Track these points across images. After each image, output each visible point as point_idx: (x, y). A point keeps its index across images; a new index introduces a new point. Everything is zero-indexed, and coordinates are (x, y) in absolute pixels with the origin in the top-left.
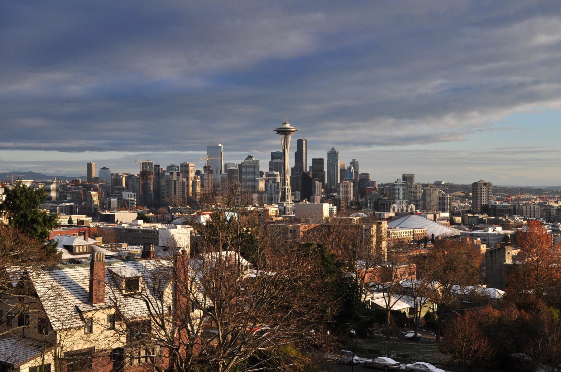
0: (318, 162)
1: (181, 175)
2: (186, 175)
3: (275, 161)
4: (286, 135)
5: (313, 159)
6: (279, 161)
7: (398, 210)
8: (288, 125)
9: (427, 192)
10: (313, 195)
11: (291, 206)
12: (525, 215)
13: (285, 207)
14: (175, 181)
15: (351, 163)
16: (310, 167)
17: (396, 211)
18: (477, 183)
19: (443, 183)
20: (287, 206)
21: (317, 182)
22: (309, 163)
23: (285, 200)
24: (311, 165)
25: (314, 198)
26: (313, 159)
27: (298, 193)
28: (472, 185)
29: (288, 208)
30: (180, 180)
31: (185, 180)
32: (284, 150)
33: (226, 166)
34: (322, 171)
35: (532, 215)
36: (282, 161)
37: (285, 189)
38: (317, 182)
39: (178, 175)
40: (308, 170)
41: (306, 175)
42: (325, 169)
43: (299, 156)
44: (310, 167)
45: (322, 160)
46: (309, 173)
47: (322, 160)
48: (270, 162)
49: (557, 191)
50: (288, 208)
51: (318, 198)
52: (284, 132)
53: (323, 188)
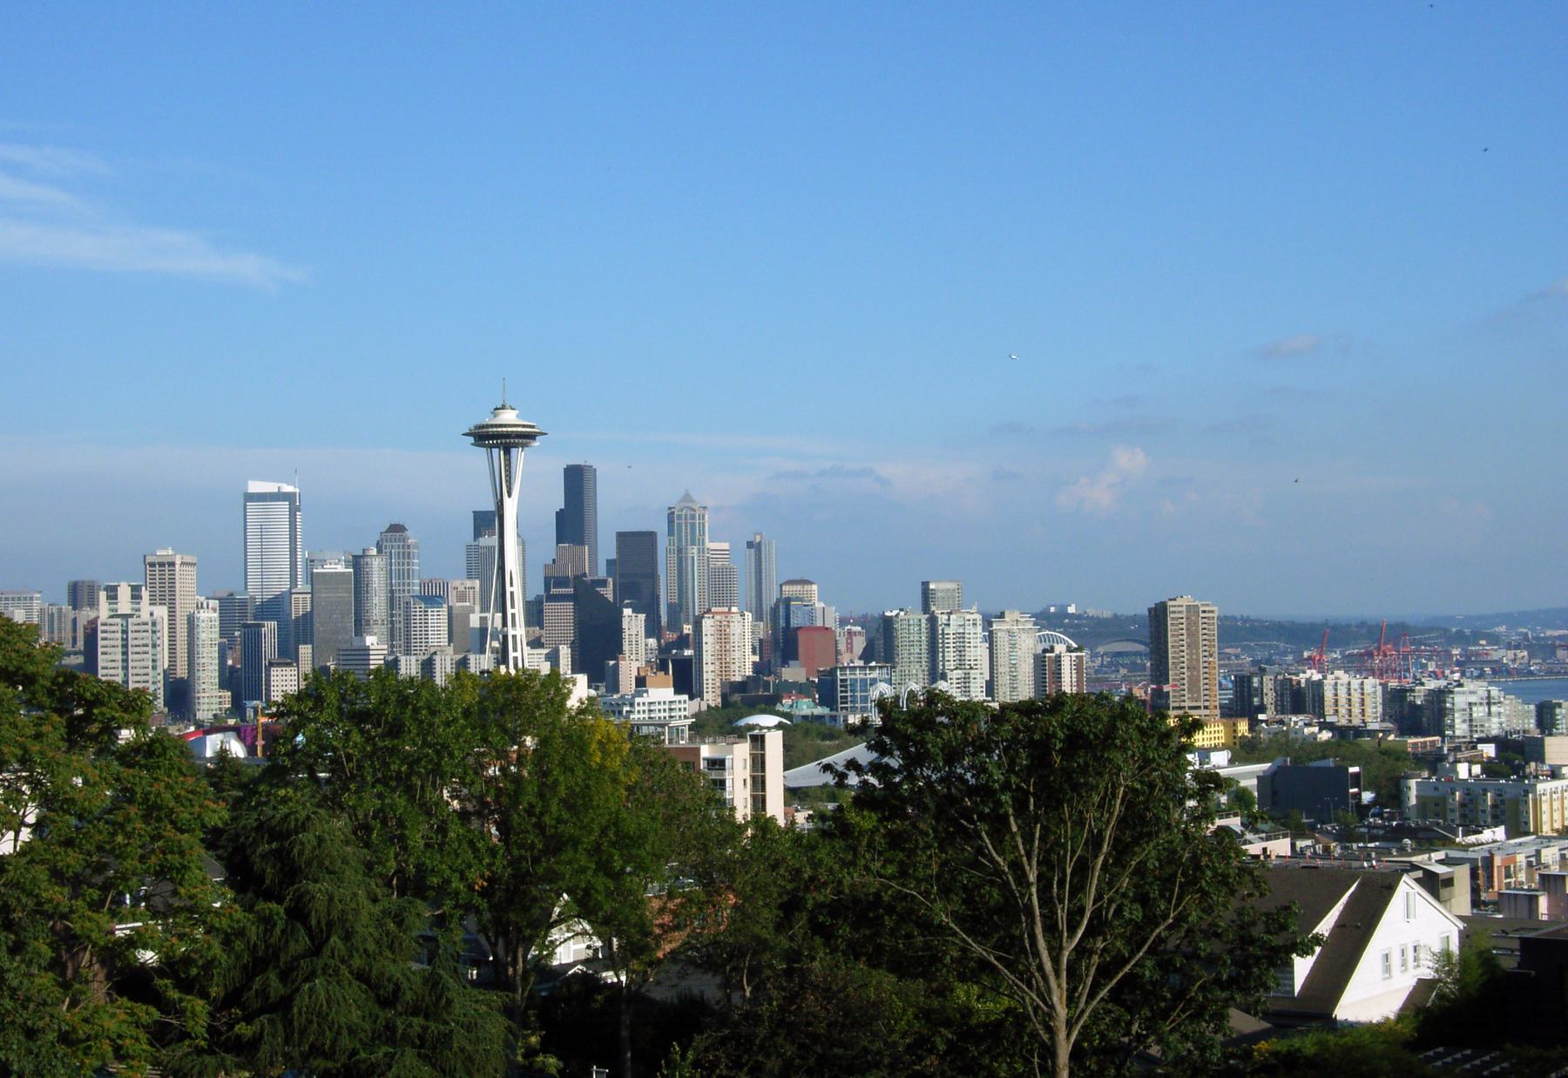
0: (636, 546)
1: (145, 594)
2: (165, 595)
4: (507, 452)
5: (621, 536)
8: (509, 417)
9: (1002, 640)
10: (616, 658)
12: (1329, 709)
14: (125, 617)
15: (750, 545)
19: (1071, 610)
21: (627, 612)
22: (607, 549)
24: (613, 555)
25: (616, 667)
26: (621, 536)
27: (565, 653)
30: (145, 616)
31: (162, 612)
33: (311, 562)
34: (653, 576)
35: (1356, 710)
36: (493, 541)
38: (627, 612)
39: (136, 596)
40: (602, 573)
43: (573, 522)
44: (610, 563)
46: (603, 583)
49: (1460, 632)
51: (629, 667)
53: (653, 629)
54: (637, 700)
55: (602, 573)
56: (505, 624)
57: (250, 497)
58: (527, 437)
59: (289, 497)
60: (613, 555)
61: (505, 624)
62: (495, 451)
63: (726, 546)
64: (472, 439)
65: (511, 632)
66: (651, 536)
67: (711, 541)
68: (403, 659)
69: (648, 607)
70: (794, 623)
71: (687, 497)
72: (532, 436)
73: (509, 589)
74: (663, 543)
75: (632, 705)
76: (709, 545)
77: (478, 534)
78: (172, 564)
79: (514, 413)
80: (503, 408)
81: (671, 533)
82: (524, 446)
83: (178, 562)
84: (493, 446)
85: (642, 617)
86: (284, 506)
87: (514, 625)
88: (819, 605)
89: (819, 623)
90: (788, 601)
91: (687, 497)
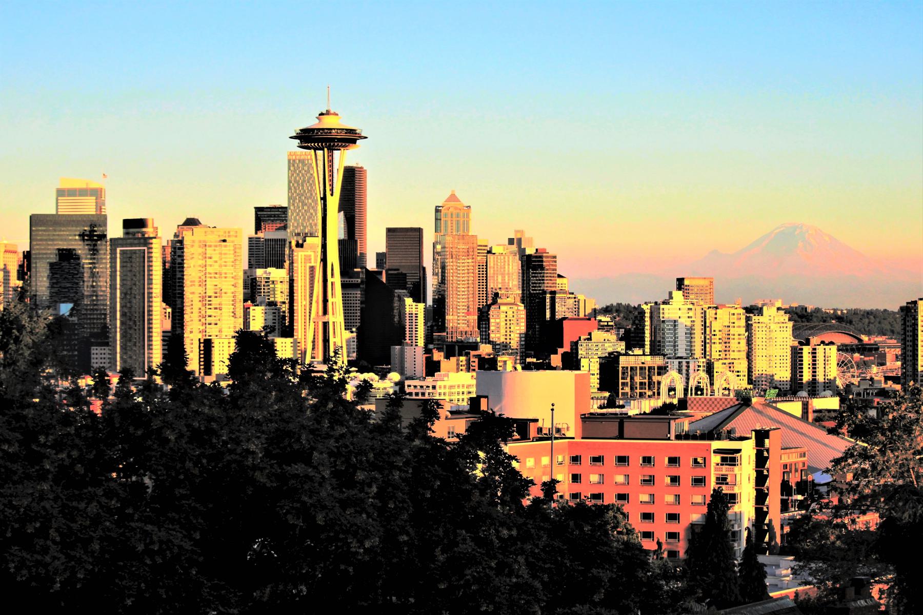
0: (405, 239)
5: (390, 231)
7: (686, 390)
15: (511, 241)
16: (378, 255)
17: (680, 394)
18: (915, 303)
22: (374, 244)
25: (402, 353)
26: (390, 231)
28: (902, 309)
32: (324, 199)
40: (371, 265)
42: (428, 261)
44: (378, 255)
45: (419, 231)
47: (419, 231)
56: (325, 312)
57: (61, 193)
59: (97, 193)
60: (383, 249)
61: (325, 312)
62: (320, 153)
65: (330, 318)
69: (419, 296)
70: (558, 316)
71: (453, 198)
72: (354, 141)
74: (429, 238)
75: (434, 387)
77: (258, 228)
80: (328, 113)
84: (315, 149)
85: (421, 306)
86: (92, 200)
91: (453, 198)
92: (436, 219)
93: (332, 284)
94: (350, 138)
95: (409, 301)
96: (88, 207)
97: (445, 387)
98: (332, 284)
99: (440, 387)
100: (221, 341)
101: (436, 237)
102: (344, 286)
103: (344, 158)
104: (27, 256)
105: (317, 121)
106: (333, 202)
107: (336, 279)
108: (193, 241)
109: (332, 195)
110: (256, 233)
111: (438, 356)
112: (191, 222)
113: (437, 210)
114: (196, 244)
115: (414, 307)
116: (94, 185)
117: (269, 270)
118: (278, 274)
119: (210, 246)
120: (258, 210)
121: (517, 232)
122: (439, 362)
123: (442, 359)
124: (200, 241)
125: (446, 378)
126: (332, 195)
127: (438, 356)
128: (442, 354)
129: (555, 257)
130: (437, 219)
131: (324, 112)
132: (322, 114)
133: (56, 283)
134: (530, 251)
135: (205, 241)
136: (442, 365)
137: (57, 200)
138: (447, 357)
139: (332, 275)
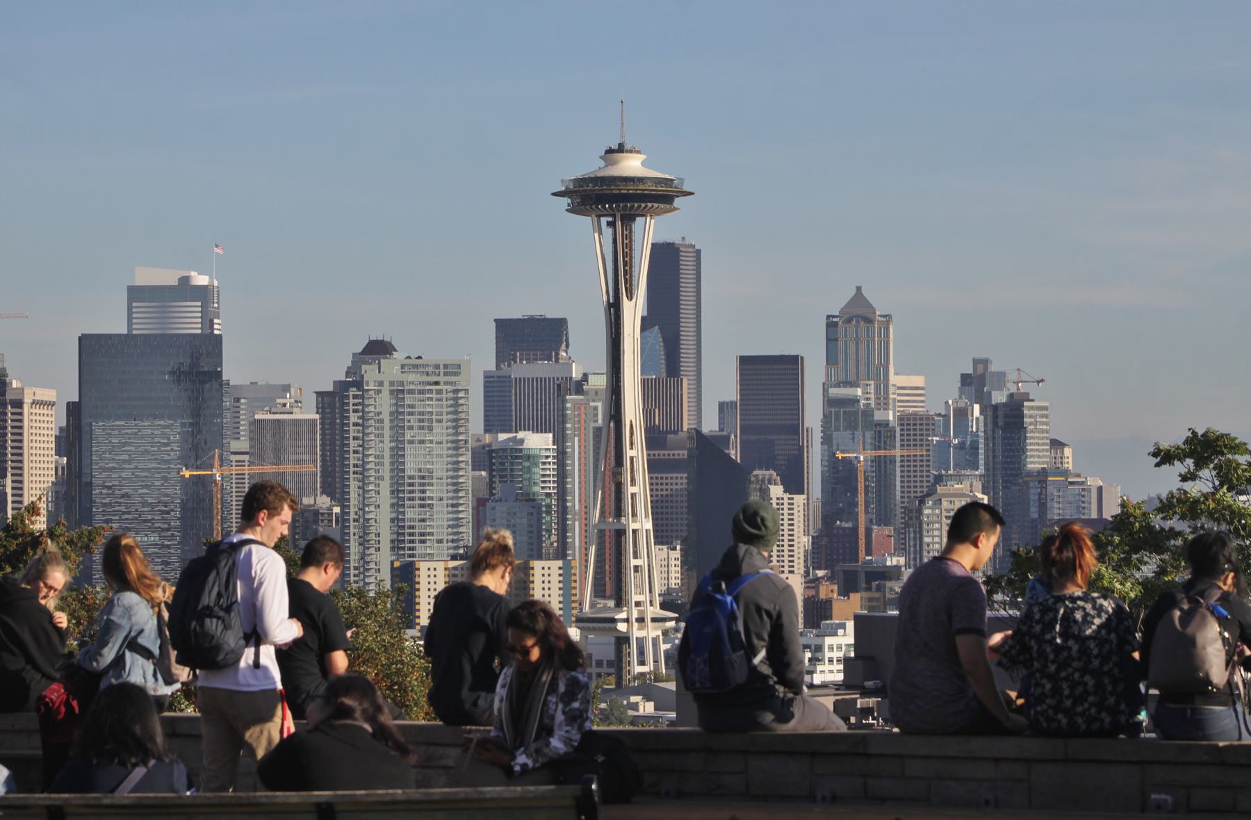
0: (770, 376)
3: (522, 369)
4: (628, 219)
5: (744, 361)
6: (541, 369)
8: (632, 165)
11: (653, 632)
13: (623, 640)
15: (966, 380)
16: (722, 406)
20: (637, 633)
23: (620, 602)
26: (744, 361)
29: (641, 643)
37: (620, 533)
41: (707, 449)
48: (487, 376)
50: (641, 643)
52: (608, 199)
54: (829, 641)
55: (710, 425)
56: (619, 512)
57: (136, 294)
58: (660, 196)
59: (203, 294)
63: (919, 381)
64: (566, 201)
66: (791, 365)
67: (896, 374)
68: (423, 566)
69: (794, 484)
73: (629, 453)
75: (819, 648)
76: (894, 379)
78: (19, 404)
79: (643, 157)
80: (621, 149)
81: (831, 359)
82: (654, 213)
83: (27, 400)
85: (799, 499)
87: (634, 515)
88: (1093, 482)
89: (1094, 515)
90: (1043, 473)
92: (828, 340)
93: (632, 459)
94: (660, 196)
95: (776, 491)
96: (189, 322)
97: (839, 647)
98: (632, 459)
99: (831, 648)
100: (432, 565)
101: (828, 375)
102: (654, 466)
103: (650, 231)
104: (74, 410)
105: (602, 163)
106: (634, 311)
107: (636, 452)
108: (381, 384)
109: (630, 298)
110: (498, 366)
111: (828, 591)
112: (378, 349)
113: (831, 325)
114: (386, 389)
115: (786, 501)
116: (201, 280)
117: (521, 435)
118: (538, 442)
119: (411, 392)
120: (504, 327)
121: (976, 362)
122: (829, 602)
123: (835, 596)
124: (392, 383)
125: (840, 632)
126: (630, 298)
127: (828, 591)
128: (836, 587)
129: (459, 366)
130: (831, 340)
131: (615, 147)
132: (610, 151)
133: (129, 462)
134: (999, 397)
135: (402, 384)
136: (836, 607)
137: (130, 308)
138: (846, 591)
139: (632, 444)
